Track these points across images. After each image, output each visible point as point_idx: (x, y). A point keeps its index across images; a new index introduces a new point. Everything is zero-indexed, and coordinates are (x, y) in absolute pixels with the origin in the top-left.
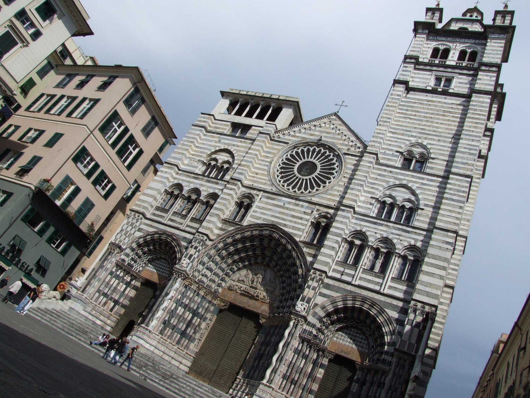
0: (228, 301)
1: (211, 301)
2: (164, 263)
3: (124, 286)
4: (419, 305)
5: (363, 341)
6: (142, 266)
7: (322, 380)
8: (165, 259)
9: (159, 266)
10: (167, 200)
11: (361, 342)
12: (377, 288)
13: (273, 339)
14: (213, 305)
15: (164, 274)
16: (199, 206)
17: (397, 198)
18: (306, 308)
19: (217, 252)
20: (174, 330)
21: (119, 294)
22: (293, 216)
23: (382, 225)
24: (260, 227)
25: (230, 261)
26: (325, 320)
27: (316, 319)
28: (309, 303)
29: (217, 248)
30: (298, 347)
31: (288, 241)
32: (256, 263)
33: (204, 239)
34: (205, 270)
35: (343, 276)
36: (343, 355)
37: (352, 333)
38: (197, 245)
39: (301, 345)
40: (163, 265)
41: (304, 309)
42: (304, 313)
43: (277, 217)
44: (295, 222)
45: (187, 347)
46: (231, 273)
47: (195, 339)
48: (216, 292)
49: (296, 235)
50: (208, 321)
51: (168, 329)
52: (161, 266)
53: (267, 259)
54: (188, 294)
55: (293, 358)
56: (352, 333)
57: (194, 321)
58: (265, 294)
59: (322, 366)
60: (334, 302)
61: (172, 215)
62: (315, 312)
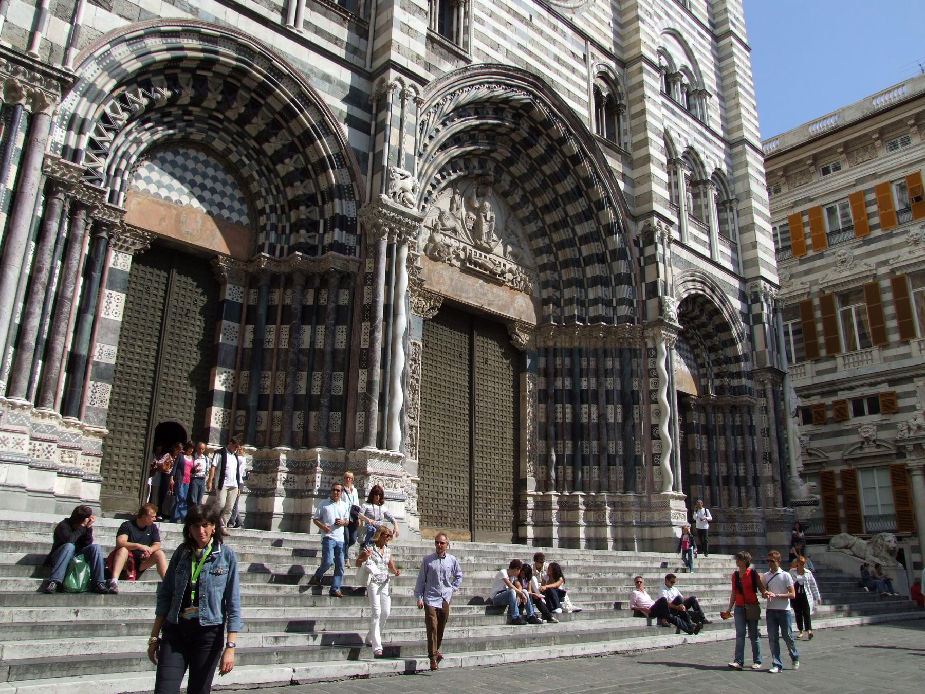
0: (438, 294)
2: (206, 164)
4: (768, 286)
12: (707, 254)
15: (225, 213)
17: (676, 61)
22: (558, 59)
23: (681, 117)
40: (205, 176)
43: (530, 54)
44: (568, 79)
52: (199, 179)
58: (514, 267)
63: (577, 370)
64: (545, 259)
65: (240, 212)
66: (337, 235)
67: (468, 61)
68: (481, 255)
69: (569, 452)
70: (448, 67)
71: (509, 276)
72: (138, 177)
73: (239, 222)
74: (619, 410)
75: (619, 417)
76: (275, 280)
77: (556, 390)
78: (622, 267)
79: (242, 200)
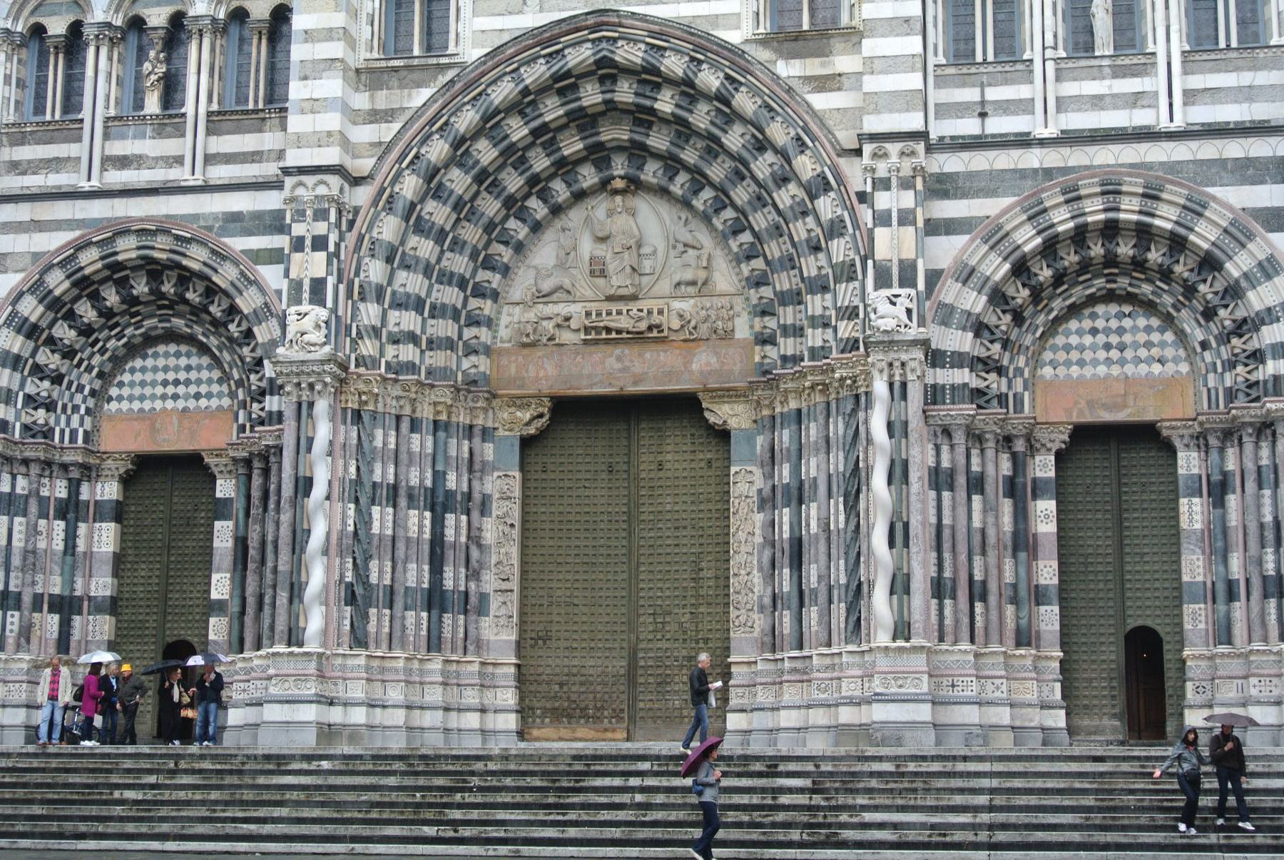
0: (538, 396)
1: (471, 427)
2: (178, 355)
3: (59, 526)
5: (1155, 337)
6: (88, 411)
7: (1060, 538)
8: (172, 336)
9: (160, 376)
10: (30, 76)
11: (1149, 345)
12: (1141, 118)
13: (812, 467)
14: (487, 434)
16: (213, 50)
18: (913, 306)
19: (407, 219)
20: (399, 604)
21: (57, 569)
25: (471, 234)
26: (991, 319)
27: (964, 329)
28: (914, 285)
29: (400, 206)
30: (938, 462)
31: (693, 59)
32: (580, 196)
33: (335, 192)
34: (394, 315)
35: (988, 121)
37: (1100, 324)
38: (321, 228)
39: (945, 449)
40: (177, 369)
41: (909, 311)
42: (914, 332)
45: (471, 642)
46: (495, 280)
47: (483, 597)
48: (475, 382)
49: (715, 19)
50: (497, 508)
51: (373, 611)
52: (171, 376)
53: (619, 166)
54: (378, 443)
56: (1100, 324)
57: (450, 534)
59: (1038, 489)
60: (995, 236)
61: (106, 136)
62: (941, 305)
63: (794, 448)
64: (745, 269)
65: (220, 395)
66: (272, 403)
67: (463, 66)
68: (609, 313)
69: (786, 588)
70: (422, 95)
71: (676, 324)
72: (110, 399)
73: (220, 408)
74: (841, 507)
75: (842, 518)
76: (248, 462)
77: (774, 486)
78: (839, 249)
79: (220, 381)
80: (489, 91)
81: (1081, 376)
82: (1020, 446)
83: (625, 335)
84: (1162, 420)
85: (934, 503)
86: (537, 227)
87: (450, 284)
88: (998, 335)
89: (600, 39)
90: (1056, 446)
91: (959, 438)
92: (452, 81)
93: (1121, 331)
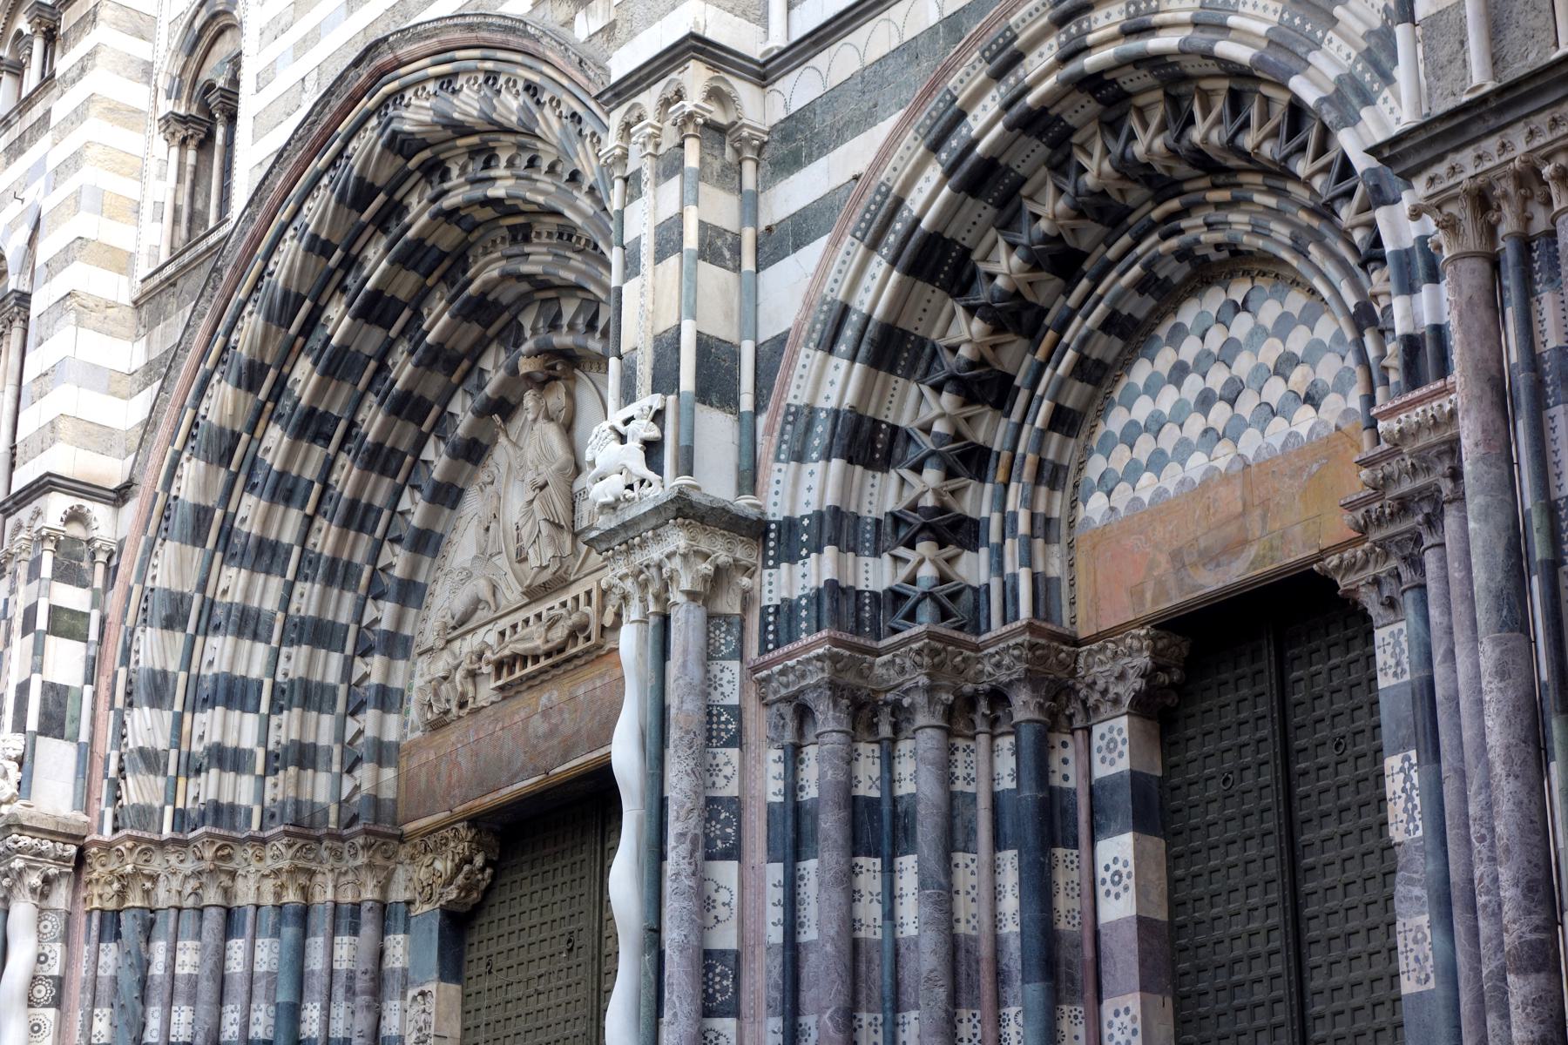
1: (356, 908)
5: (1298, 341)
11: (1284, 366)
24: (316, 150)
30: (793, 786)
36: (1212, 581)
42: (660, 489)
54: (158, 969)
55: (792, 903)
56: (1190, 349)
80: (271, 267)
81: (1160, 493)
82: (1024, 705)
83: (543, 662)
84: (1322, 554)
85: (778, 894)
86: (447, 495)
87: (299, 643)
88: (928, 444)
89: (383, 103)
90: (1126, 691)
91: (828, 718)
92: (216, 270)
93: (1230, 350)
